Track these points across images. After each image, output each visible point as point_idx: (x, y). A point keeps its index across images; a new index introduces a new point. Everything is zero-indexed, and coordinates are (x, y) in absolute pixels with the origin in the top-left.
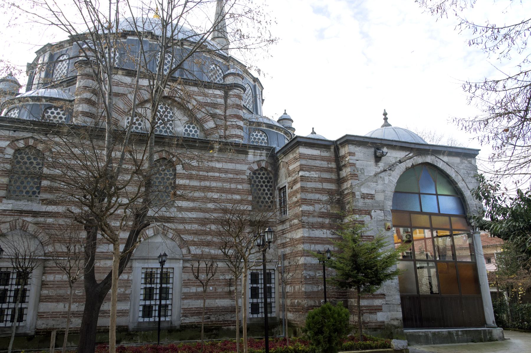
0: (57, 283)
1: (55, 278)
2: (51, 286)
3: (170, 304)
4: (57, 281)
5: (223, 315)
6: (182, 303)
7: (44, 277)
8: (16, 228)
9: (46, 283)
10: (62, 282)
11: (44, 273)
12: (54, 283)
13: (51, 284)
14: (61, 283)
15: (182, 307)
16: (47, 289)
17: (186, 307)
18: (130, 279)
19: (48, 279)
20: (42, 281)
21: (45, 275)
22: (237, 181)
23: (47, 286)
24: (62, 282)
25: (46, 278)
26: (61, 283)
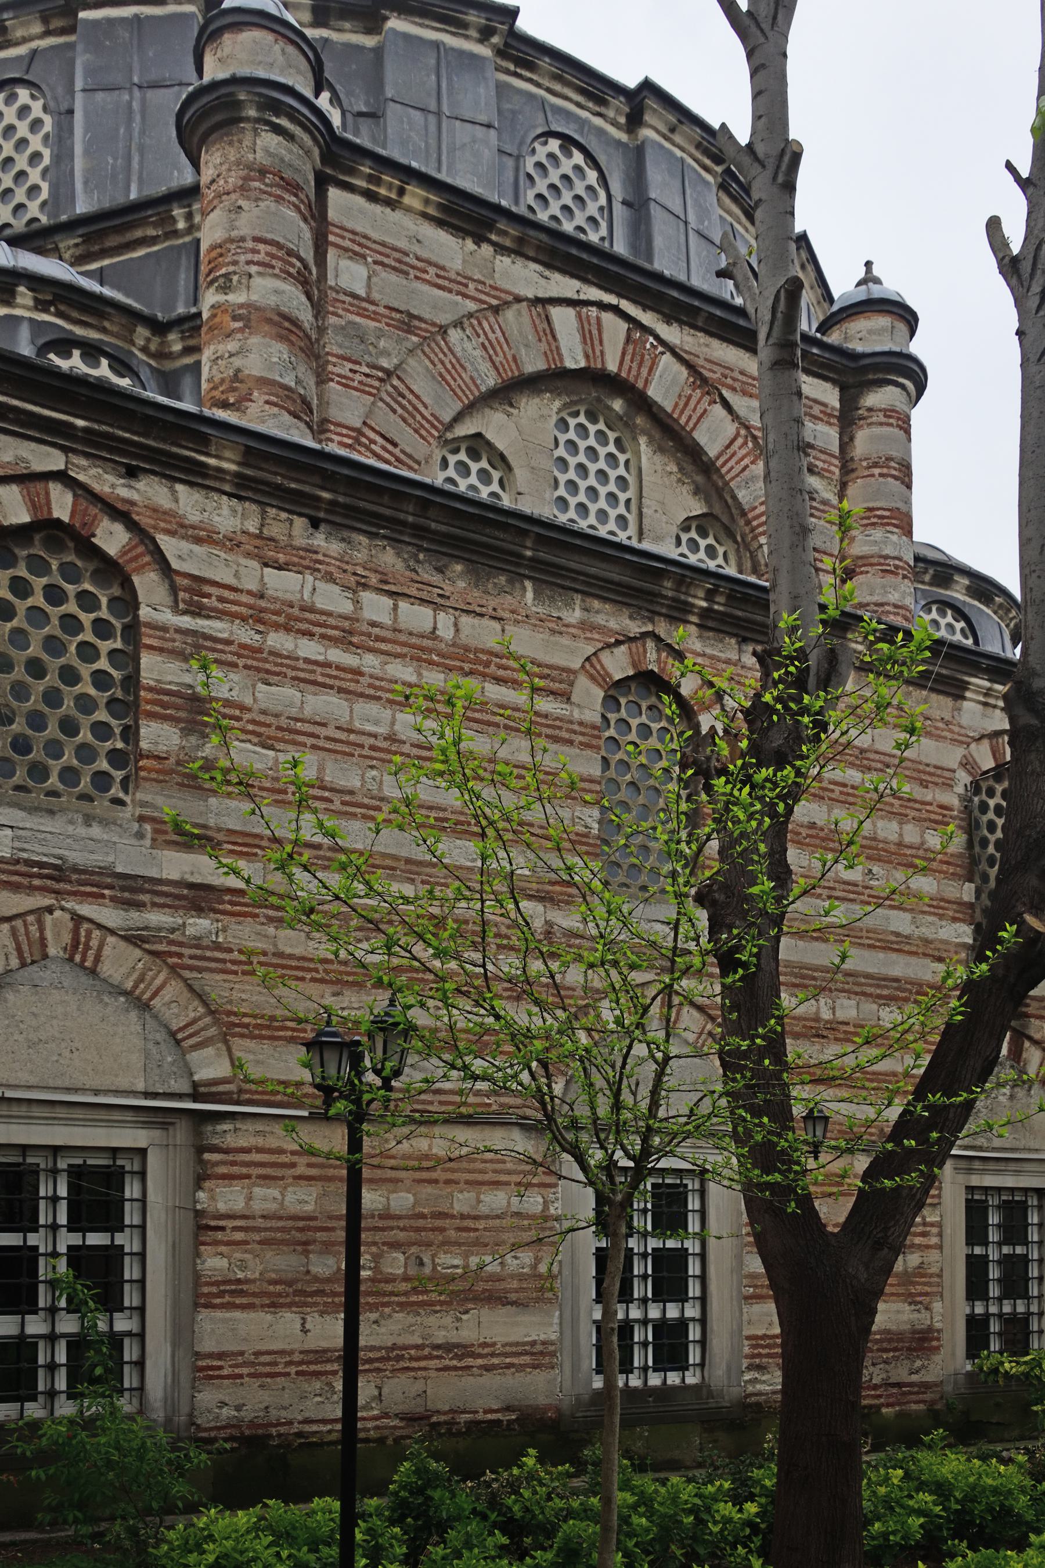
0: (260, 1222)
1: (249, 1198)
2: (239, 1236)
3: (693, 1319)
4: (263, 1217)
5: (886, 1362)
6: (745, 1317)
7: (201, 1195)
8: (45, 956)
9: (213, 1223)
10: (280, 1218)
11: (200, 1180)
12: (250, 1223)
13: (235, 1229)
14: (281, 1224)
15: (746, 1332)
16: (223, 1249)
17: (760, 1333)
18: (552, 1211)
19: (222, 1207)
20: (199, 1214)
21: (207, 1184)
22: (925, 815)
23: (219, 1235)
24: (280, 1218)
25: (213, 1198)
26: (281, 1224)
